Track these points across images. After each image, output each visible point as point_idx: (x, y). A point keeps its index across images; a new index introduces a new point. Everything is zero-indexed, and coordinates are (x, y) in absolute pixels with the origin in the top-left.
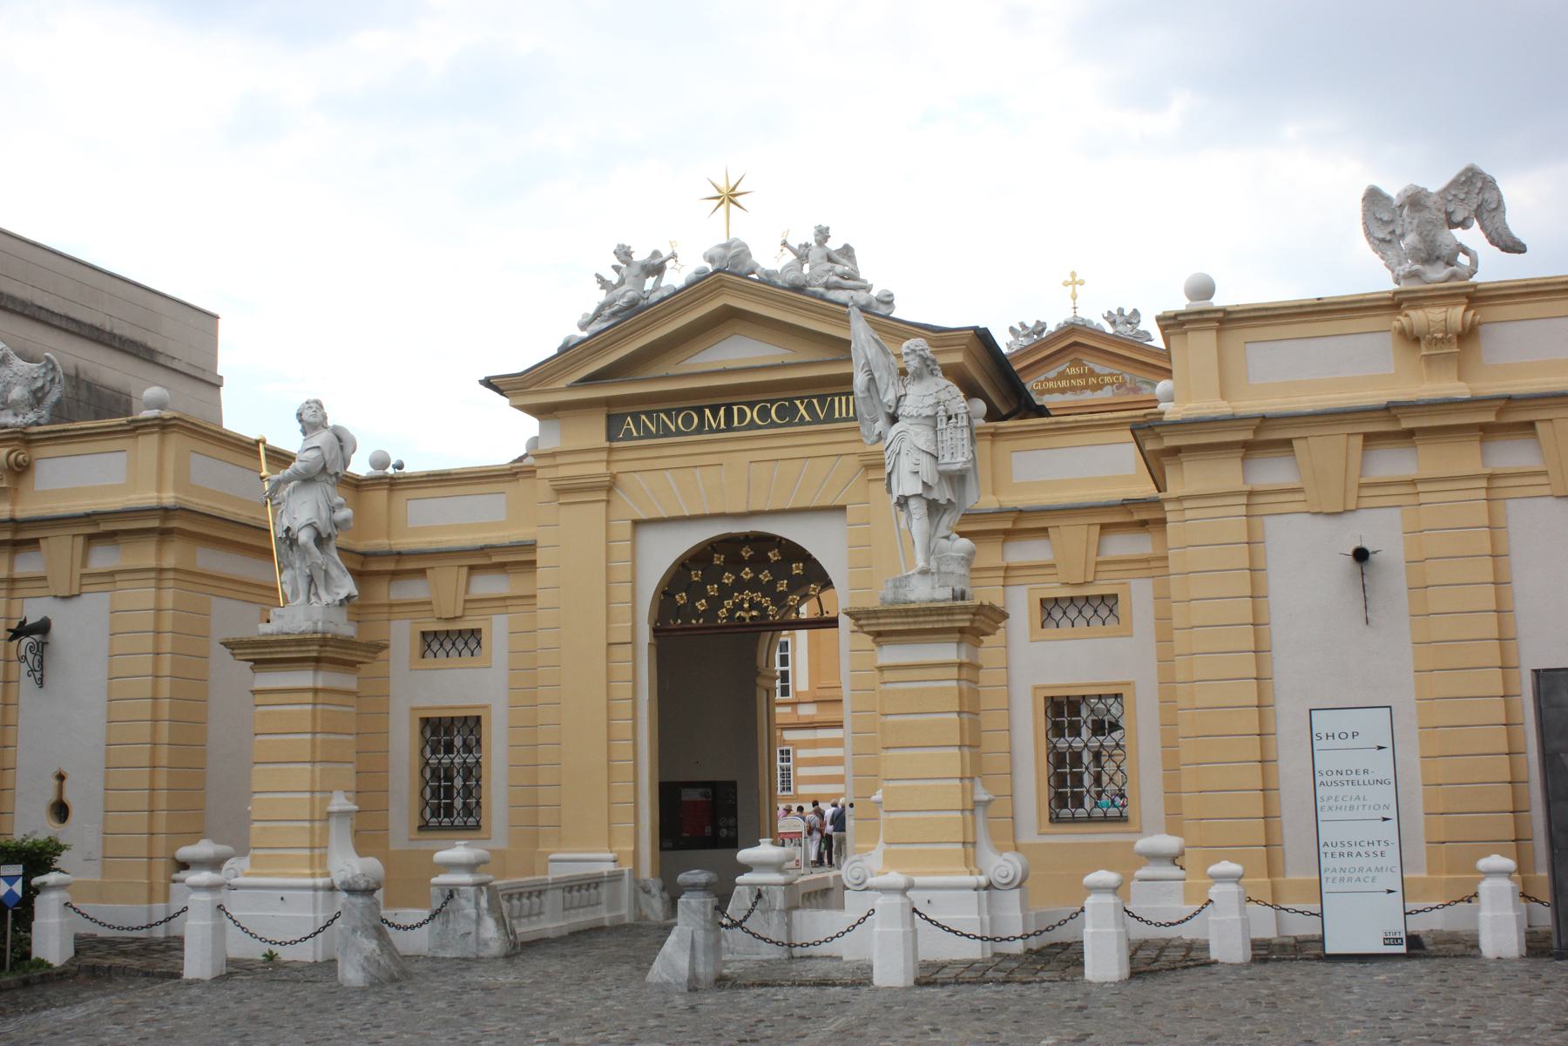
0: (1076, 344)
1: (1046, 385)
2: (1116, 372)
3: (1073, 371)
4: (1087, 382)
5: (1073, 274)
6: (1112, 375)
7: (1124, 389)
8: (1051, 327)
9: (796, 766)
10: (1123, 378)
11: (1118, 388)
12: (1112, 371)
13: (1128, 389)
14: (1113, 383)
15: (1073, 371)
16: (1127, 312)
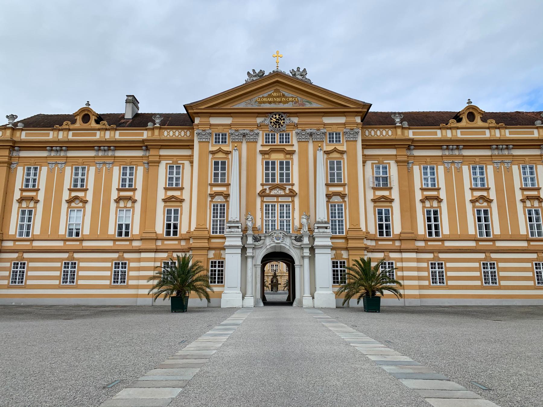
0: (278, 82)
1: (262, 100)
2: (294, 96)
3: (275, 94)
4: (281, 99)
5: (278, 52)
6: (292, 97)
7: (297, 104)
8: (266, 73)
9: (129, 271)
10: (298, 99)
11: (295, 103)
12: (293, 96)
13: (299, 104)
14: (293, 101)
15: (275, 94)
16: (301, 70)
